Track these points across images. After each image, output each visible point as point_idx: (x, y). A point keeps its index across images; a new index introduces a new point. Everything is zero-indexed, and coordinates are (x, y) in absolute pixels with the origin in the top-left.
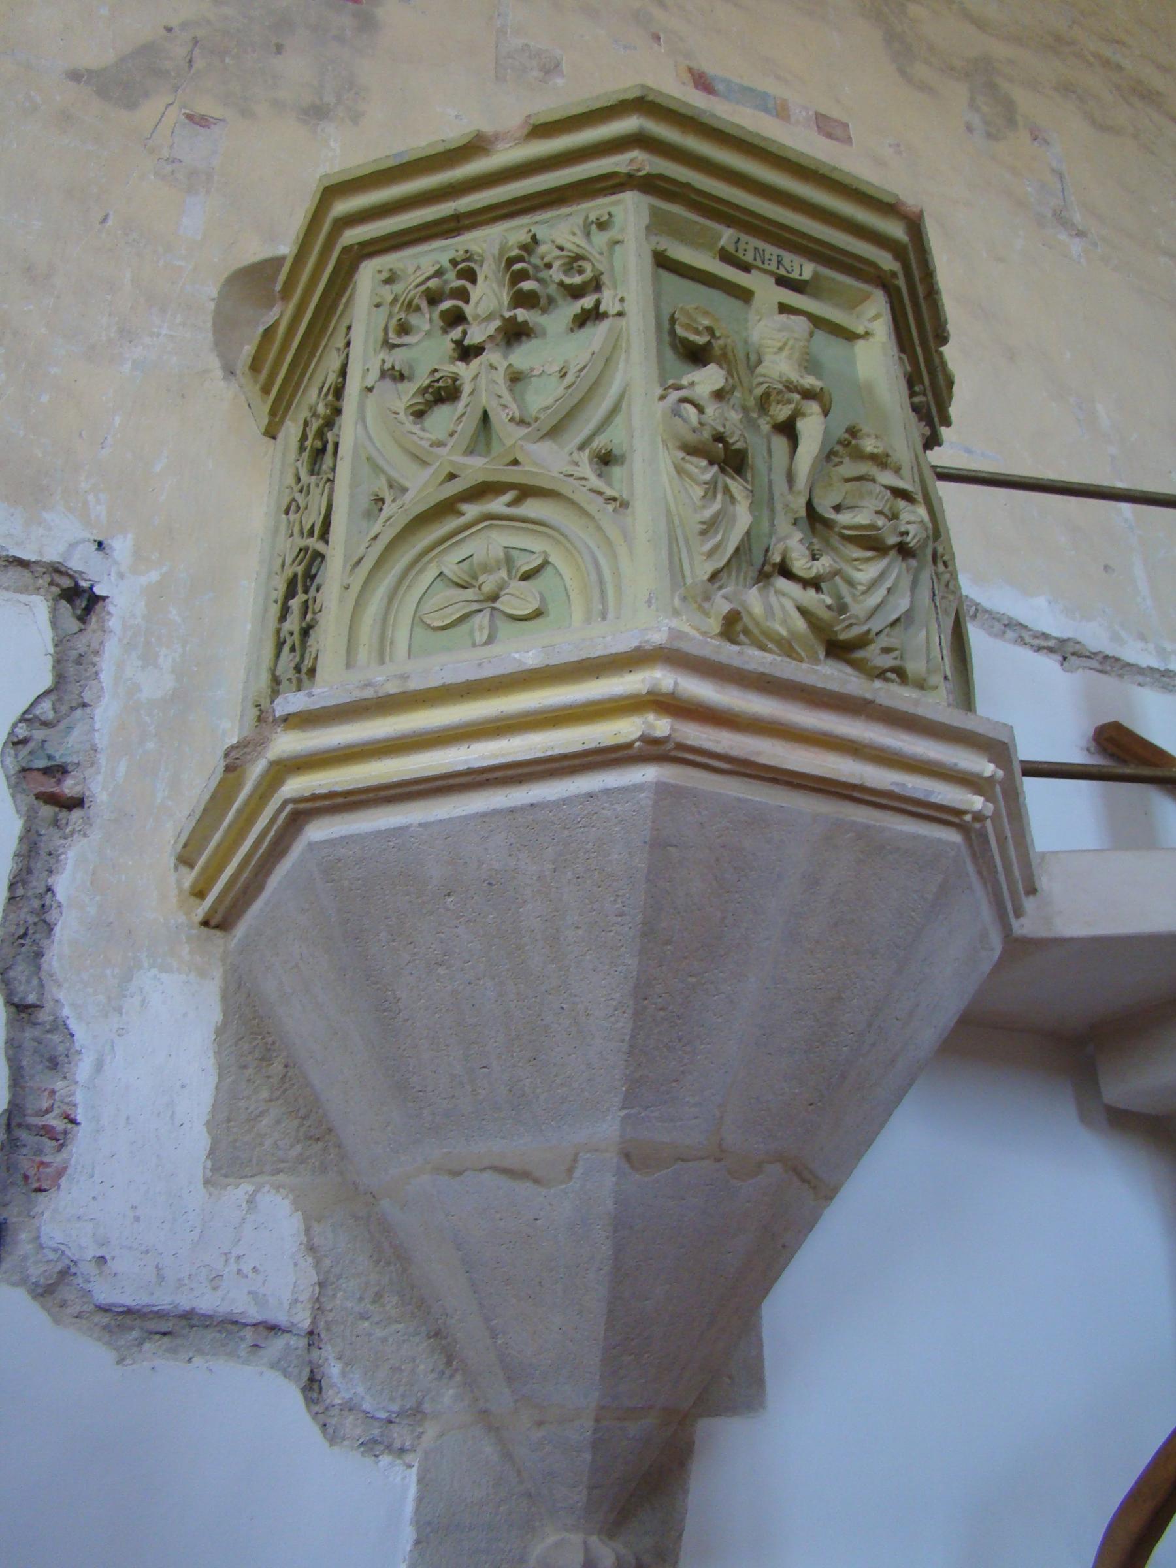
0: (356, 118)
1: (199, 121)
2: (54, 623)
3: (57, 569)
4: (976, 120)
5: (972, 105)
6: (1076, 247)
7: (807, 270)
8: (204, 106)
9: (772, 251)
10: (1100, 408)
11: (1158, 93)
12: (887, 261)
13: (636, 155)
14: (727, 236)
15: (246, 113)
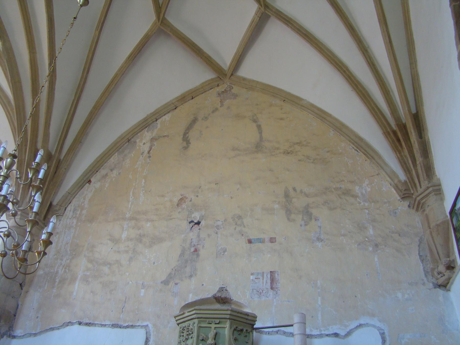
0: (196, 275)
1: (176, 284)
4: (303, 223)
5: (303, 219)
6: (319, 244)
7: (217, 321)
8: (177, 282)
9: (213, 320)
10: (318, 282)
11: (350, 190)
12: (228, 316)
14: (208, 320)
15: (182, 280)
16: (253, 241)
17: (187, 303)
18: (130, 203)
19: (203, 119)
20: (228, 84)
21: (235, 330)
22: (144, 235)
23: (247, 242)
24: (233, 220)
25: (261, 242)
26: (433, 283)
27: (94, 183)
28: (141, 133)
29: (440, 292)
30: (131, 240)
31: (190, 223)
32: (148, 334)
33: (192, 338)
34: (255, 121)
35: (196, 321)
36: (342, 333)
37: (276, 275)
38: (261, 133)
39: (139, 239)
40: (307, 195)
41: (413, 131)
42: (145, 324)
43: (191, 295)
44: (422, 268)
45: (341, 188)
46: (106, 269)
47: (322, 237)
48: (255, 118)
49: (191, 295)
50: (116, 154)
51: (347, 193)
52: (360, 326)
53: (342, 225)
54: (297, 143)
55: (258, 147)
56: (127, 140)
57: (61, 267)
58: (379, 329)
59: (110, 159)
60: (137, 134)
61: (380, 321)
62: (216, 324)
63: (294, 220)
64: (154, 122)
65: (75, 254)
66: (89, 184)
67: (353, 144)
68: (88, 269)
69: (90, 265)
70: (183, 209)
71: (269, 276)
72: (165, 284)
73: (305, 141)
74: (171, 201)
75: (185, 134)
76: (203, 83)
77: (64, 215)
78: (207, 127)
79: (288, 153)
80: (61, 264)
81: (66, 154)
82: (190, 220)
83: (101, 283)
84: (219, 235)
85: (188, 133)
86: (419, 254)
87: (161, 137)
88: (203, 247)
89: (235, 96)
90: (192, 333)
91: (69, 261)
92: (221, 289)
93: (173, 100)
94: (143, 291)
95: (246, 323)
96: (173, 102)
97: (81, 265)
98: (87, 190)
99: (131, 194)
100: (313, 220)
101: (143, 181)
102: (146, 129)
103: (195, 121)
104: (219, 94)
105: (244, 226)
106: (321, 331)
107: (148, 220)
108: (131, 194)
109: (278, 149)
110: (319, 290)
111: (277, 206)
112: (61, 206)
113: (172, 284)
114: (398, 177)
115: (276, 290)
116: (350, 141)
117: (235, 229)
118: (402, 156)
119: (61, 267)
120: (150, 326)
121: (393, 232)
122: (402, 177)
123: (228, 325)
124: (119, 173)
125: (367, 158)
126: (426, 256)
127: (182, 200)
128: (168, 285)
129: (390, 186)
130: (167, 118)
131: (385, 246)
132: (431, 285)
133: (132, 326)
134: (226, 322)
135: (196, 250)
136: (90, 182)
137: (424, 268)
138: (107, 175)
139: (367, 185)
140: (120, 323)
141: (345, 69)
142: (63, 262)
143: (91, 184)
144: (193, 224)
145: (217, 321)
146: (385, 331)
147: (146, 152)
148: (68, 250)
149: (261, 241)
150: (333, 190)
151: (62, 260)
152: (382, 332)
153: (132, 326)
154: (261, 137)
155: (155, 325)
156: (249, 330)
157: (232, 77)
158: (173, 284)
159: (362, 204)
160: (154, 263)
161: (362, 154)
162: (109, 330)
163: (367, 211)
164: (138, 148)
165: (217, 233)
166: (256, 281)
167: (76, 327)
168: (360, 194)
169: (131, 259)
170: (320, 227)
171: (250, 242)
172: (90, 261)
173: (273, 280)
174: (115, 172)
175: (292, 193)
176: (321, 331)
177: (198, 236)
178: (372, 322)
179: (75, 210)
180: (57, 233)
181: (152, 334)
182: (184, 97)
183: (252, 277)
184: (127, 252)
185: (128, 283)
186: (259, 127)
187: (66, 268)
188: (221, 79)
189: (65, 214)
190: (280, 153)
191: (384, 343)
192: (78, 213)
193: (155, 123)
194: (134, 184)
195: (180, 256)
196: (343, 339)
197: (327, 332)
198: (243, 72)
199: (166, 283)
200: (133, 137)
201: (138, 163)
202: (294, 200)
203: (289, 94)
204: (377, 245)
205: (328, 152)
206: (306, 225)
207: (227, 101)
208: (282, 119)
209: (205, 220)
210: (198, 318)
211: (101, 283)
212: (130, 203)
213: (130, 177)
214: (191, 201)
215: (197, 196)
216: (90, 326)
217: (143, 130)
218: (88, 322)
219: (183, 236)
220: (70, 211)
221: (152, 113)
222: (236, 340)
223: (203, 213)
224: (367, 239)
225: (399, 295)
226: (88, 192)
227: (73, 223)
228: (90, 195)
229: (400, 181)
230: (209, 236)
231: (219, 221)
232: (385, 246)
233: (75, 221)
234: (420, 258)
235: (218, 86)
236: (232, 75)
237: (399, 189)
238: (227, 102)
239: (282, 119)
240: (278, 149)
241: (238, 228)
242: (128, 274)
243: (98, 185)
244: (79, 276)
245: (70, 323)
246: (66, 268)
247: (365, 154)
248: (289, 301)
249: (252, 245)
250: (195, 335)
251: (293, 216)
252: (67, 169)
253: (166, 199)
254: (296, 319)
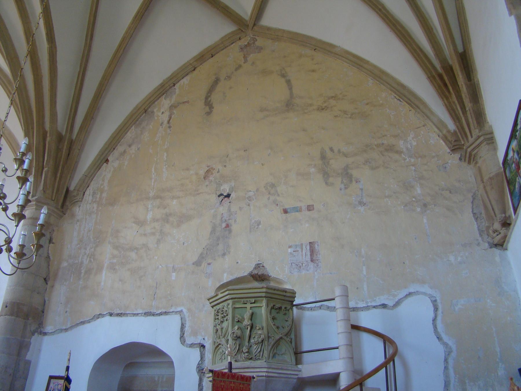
0: (229, 252)
1: (209, 264)
2: (200, 351)
3: (200, 343)
4: (342, 186)
5: (342, 182)
6: (362, 209)
7: (253, 300)
8: (210, 261)
9: (248, 299)
10: (362, 250)
13: (229, 296)
14: (242, 300)
15: (215, 260)
16: (289, 210)
17: (222, 283)
18: (153, 180)
19: (225, 79)
20: (252, 36)
21: (272, 308)
22: (170, 214)
23: (282, 212)
24: (266, 189)
25: (297, 212)
26: (489, 243)
27: (112, 162)
28: (158, 101)
29: (497, 251)
30: (157, 220)
31: (219, 196)
32: (183, 320)
33: (227, 320)
34: (283, 76)
35: (230, 302)
36: (391, 303)
37: (316, 246)
38: (291, 89)
39: (166, 219)
40: (346, 155)
41: (460, 73)
42: (179, 309)
43: (225, 275)
44: (476, 226)
45: (383, 144)
46: (133, 255)
47: (364, 200)
48: (283, 72)
49: (225, 275)
50: (133, 127)
51: (390, 149)
52: (410, 294)
53: (386, 185)
54: (332, 97)
55: (289, 105)
56: (143, 111)
57: (85, 257)
58: (430, 296)
59: (126, 133)
60: (154, 103)
61: (431, 288)
62: (251, 303)
63: (332, 184)
64: (171, 87)
66: (107, 163)
67: (395, 93)
68: (114, 257)
69: (116, 252)
70: (211, 181)
71: (308, 247)
72: (197, 265)
73: (341, 94)
74: (197, 174)
75: (206, 98)
76: (222, 38)
77: (84, 200)
78: (231, 88)
79: (323, 109)
81: (78, 133)
82: (219, 193)
83: (129, 270)
84: (252, 207)
85: (210, 96)
86: (472, 211)
87: (181, 103)
88: (235, 221)
89: (260, 49)
90: (227, 315)
91: (93, 250)
92: (258, 266)
93: (190, 60)
94: (174, 274)
95: (284, 300)
96: (191, 62)
97: (107, 253)
98: (105, 171)
99: (153, 170)
100: (354, 182)
101: (165, 154)
102: (164, 96)
103: (217, 81)
104: (241, 49)
105: (278, 195)
106: (367, 302)
107: (173, 198)
108: (153, 170)
109: (311, 105)
110: (364, 259)
111: (313, 169)
112: (78, 190)
113: (204, 264)
114: (446, 126)
115: (317, 262)
116: (391, 90)
117: (269, 199)
118: (449, 103)
119: (85, 257)
120: (185, 311)
121: (443, 190)
122: (451, 126)
123: (264, 303)
124: (138, 149)
125: (411, 108)
126: (481, 214)
127: (209, 172)
128: (201, 265)
129: (438, 138)
130: (185, 81)
131: (435, 205)
132: (487, 245)
133: (166, 313)
134: (262, 300)
135: (227, 226)
136: (107, 161)
137: (478, 227)
138: (125, 152)
139: (413, 138)
140: (152, 311)
141: (380, 7)
142: (88, 252)
143: (109, 163)
144: (222, 197)
145: (253, 300)
146: (438, 299)
147: (166, 122)
148: (91, 237)
149: (298, 210)
150: (375, 147)
151: (86, 249)
152: (434, 299)
153: (166, 312)
154: (291, 94)
155: (189, 310)
156: (289, 307)
157: (255, 28)
158: (206, 264)
159: (408, 160)
160: (184, 244)
161: (405, 103)
162: (142, 319)
163: (413, 168)
164: (156, 118)
165: (249, 205)
166: (295, 253)
167: (108, 318)
168: (404, 150)
169: (158, 242)
170: (362, 189)
171: (286, 211)
172: (116, 247)
173: (312, 252)
174: (134, 147)
175: (329, 154)
176: (367, 302)
177: (229, 210)
178: (422, 290)
179: (94, 193)
180: (78, 221)
181: (187, 319)
182: (203, 56)
183: (290, 250)
184: (153, 234)
185: (158, 267)
186: (288, 82)
187: (90, 258)
188: (242, 31)
189: (84, 199)
190: (314, 110)
191: (436, 311)
192: (98, 196)
193: (173, 88)
195: (211, 233)
196: (391, 309)
197: (374, 304)
198: (267, 21)
199: (197, 263)
200: (149, 107)
201: (157, 135)
202: (332, 162)
203: (321, 41)
204: (425, 205)
205: (367, 104)
206: (346, 188)
207: (251, 55)
208: (313, 71)
209: (235, 192)
210: (232, 299)
211: (129, 270)
212: (153, 180)
213: (151, 151)
214: (218, 172)
215: (225, 166)
216: (121, 316)
217: (160, 97)
218: (119, 312)
219: (213, 211)
220: (89, 195)
221: (169, 78)
222: (274, 319)
223: (233, 184)
224: (414, 199)
225: (452, 258)
226: (107, 172)
228: (109, 176)
229: (449, 131)
230: (240, 209)
231: (250, 191)
232: (435, 205)
233: (95, 206)
234: (474, 216)
235: (240, 39)
236: (254, 25)
237: (448, 140)
238: (251, 57)
239: (313, 71)
240: (311, 105)
241: (272, 198)
242: (156, 258)
243: (116, 164)
244: (106, 265)
246: (90, 258)
247: (409, 104)
248: (331, 273)
249: (288, 215)
250: (230, 316)
251: (331, 180)
252: (81, 150)
253: (191, 172)
254: (338, 292)
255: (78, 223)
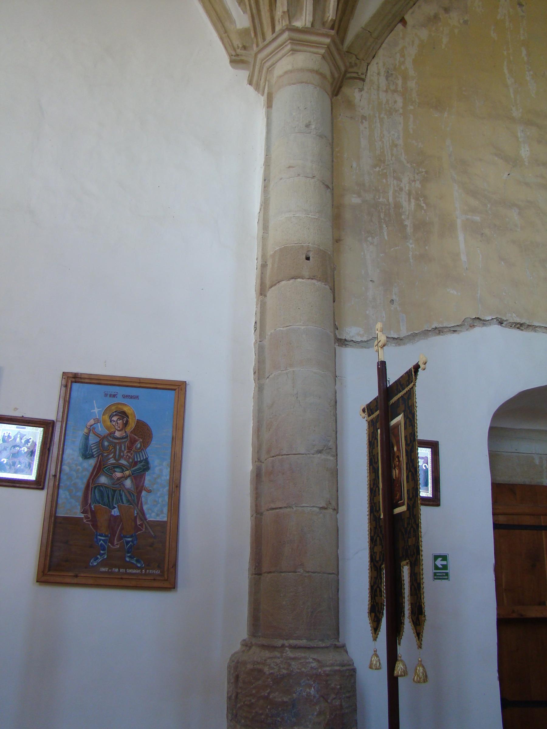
65: (426, 172)
80: (401, 189)
99: (506, 71)
101: (524, 52)
108: (506, 71)
124: (466, 22)
136: (403, 21)
167: (495, 328)
194: (505, 53)
218: (518, 320)
220: (379, 74)
227: (395, 102)
244: (459, 222)
245: (479, 321)
246: (417, 199)
255: (366, 124)
